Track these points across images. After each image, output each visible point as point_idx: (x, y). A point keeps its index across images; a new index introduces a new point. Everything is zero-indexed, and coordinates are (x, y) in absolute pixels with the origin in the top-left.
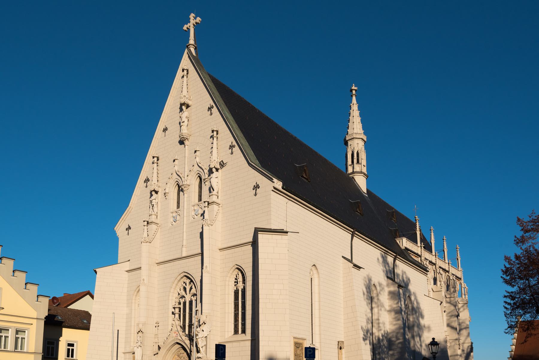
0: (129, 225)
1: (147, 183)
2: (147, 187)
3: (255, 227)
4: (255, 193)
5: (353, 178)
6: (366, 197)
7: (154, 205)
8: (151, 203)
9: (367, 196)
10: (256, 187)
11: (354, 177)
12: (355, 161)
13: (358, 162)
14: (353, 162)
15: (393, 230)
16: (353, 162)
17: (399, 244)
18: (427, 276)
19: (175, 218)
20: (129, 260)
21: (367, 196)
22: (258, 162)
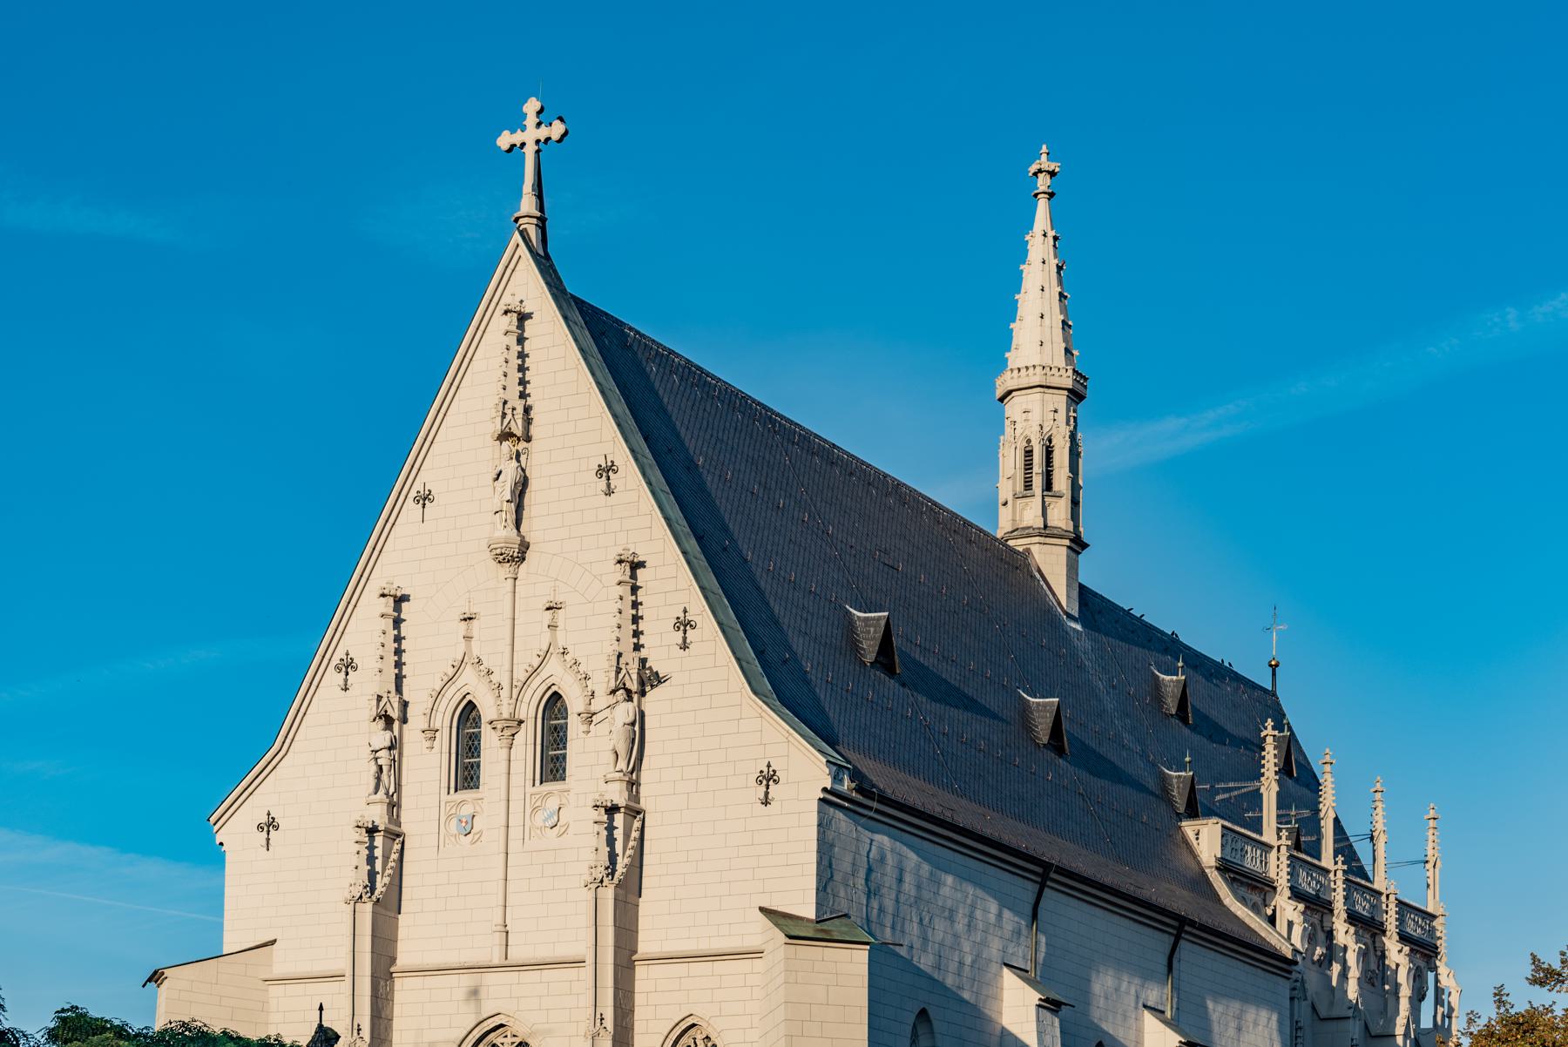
0: (269, 814)
1: (347, 674)
3: (766, 905)
4: (762, 796)
5: (1028, 550)
6: (1069, 629)
7: (385, 769)
8: (376, 759)
9: (1079, 627)
10: (768, 778)
11: (1035, 549)
12: (1038, 482)
13: (1048, 486)
14: (1028, 485)
15: (1175, 781)
16: (1028, 485)
17: (1195, 842)
18: (1289, 979)
19: (464, 824)
20: (273, 942)
21: (1079, 627)
22: (770, 688)
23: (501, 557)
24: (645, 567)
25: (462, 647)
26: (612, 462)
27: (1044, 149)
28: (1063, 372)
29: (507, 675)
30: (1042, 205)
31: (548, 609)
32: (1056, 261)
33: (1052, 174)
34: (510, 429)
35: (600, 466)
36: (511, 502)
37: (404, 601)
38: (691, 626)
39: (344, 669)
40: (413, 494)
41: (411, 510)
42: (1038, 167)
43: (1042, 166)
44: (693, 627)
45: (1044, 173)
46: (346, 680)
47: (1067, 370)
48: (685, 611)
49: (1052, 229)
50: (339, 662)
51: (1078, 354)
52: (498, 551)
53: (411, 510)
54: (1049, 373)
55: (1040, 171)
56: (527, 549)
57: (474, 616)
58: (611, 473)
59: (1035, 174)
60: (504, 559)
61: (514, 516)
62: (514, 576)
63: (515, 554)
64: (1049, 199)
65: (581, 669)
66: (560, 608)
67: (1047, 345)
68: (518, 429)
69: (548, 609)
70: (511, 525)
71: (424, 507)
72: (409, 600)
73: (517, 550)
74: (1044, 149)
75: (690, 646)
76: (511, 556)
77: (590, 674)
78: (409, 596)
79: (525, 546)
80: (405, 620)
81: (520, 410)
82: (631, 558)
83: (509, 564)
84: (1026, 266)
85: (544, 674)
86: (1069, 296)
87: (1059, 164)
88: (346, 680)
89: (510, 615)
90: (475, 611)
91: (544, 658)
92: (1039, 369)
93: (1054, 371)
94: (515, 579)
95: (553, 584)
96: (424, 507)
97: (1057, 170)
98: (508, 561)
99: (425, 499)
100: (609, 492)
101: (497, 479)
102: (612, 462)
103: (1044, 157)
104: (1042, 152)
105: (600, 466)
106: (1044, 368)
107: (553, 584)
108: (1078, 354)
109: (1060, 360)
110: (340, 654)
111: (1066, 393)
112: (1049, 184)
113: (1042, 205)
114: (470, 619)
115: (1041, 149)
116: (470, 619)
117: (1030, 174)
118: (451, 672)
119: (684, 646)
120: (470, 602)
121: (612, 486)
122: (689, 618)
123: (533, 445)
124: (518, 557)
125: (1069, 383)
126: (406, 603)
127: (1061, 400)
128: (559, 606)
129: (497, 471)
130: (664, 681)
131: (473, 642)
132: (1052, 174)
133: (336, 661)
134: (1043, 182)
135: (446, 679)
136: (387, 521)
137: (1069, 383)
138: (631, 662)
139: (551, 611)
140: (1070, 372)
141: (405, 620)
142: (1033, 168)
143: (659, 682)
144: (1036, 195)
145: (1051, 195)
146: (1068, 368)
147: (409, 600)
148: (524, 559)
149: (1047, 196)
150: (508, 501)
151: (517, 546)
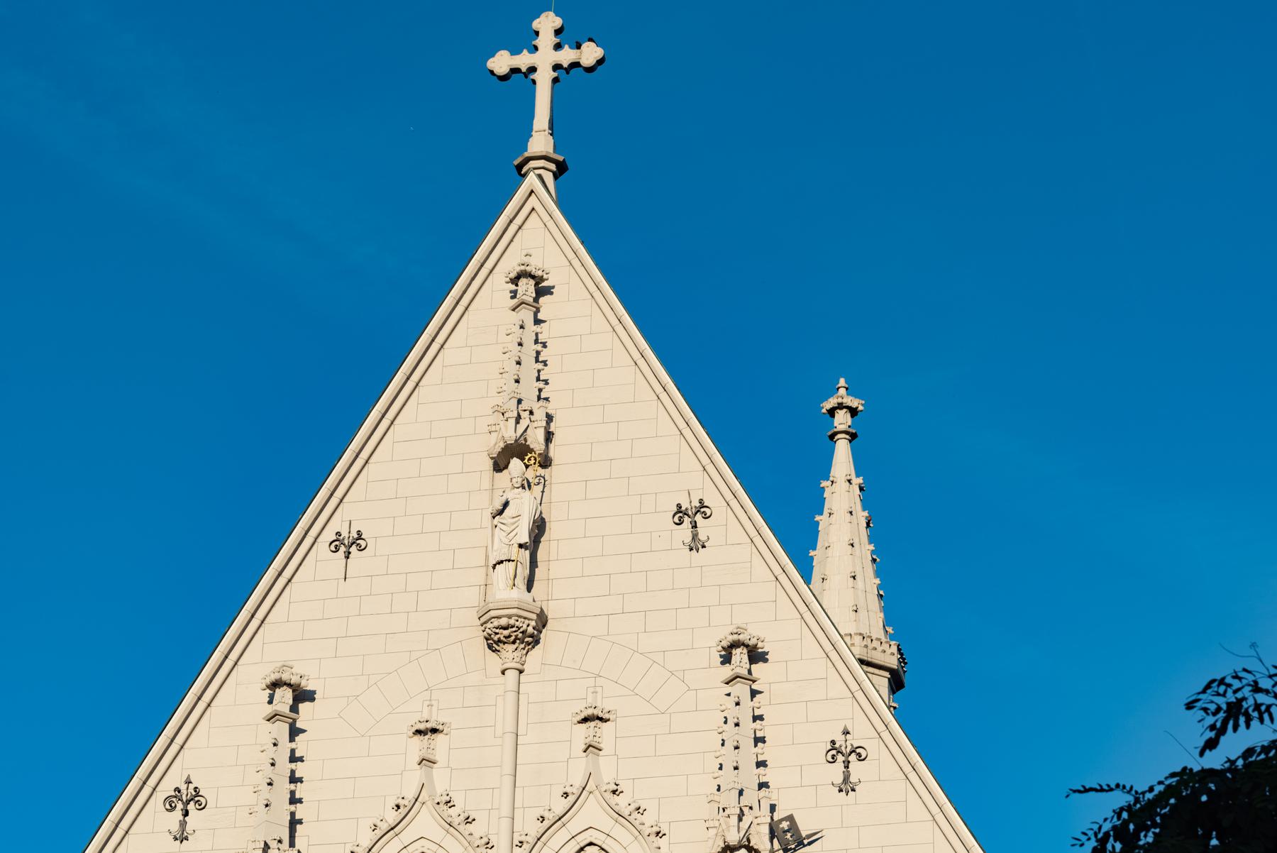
1: (186, 814)
2: (182, 838)
23: (506, 632)
24: (766, 661)
25: (416, 776)
26: (701, 501)
27: (842, 382)
28: (885, 646)
29: (505, 823)
30: (842, 448)
31: (585, 720)
32: (866, 514)
33: (853, 412)
34: (526, 440)
35: (679, 506)
36: (526, 549)
37: (303, 700)
38: (859, 755)
39: (180, 806)
40: (329, 535)
41: (323, 561)
42: (840, 400)
43: (845, 401)
44: (860, 758)
45: (845, 410)
46: (183, 824)
47: (890, 645)
48: (846, 733)
49: (858, 476)
50: (173, 794)
51: (892, 632)
52: (504, 622)
53: (323, 561)
54: (870, 646)
55: (841, 406)
56: (544, 626)
57: (440, 727)
58: (699, 518)
59: (832, 412)
60: (510, 636)
61: (528, 571)
62: (519, 666)
63: (530, 630)
64: (850, 441)
65: (649, 819)
66: (609, 720)
67: (862, 612)
68: (536, 440)
69: (585, 720)
70: (521, 583)
71: (347, 557)
72: (313, 700)
73: (533, 623)
74: (842, 382)
75: (856, 788)
76: (523, 632)
77: (664, 830)
78: (314, 692)
79: (542, 621)
80: (304, 731)
81: (540, 416)
82: (752, 643)
83: (515, 646)
84: (820, 517)
85: (575, 825)
86: (878, 560)
87: (863, 402)
88: (183, 824)
89: (510, 727)
90: (441, 720)
91: (573, 798)
92: (858, 639)
93: (876, 644)
94: (521, 672)
95: (591, 682)
96: (347, 557)
97: (861, 408)
98: (514, 642)
99: (349, 544)
100: (696, 544)
101: (501, 512)
102: (701, 501)
103: (842, 391)
104: (840, 385)
105: (679, 506)
106: (864, 638)
107: (591, 682)
108: (892, 632)
109: (878, 632)
110: (174, 780)
111: (887, 674)
112: (849, 423)
113: (842, 448)
114: (434, 731)
115: (838, 383)
116: (434, 731)
117: (824, 411)
118: (392, 817)
119: (847, 786)
120: (430, 705)
121: (702, 537)
122: (854, 741)
123: (551, 473)
124: (531, 636)
125: (893, 662)
126: (307, 704)
127: (883, 681)
128: (606, 716)
129: (503, 500)
130: (810, 844)
131: (436, 771)
132: (853, 412)
133: (166, 789)
134: (842, 420)
135: (385, 827)
136: (280, 574)
137: (893, 662)
138: (756, 806)
139: (592, 724)
140: (894, 649)
141: (304, 731)
142: (831, 402)
143: (801, 844)
144: (832, 437)
145: (853, 436)
146: (892, 643)
147: (313, 700)
148: (537, 642)
149: (848, 437)
150: (521, 546)
151: (534, 617)
